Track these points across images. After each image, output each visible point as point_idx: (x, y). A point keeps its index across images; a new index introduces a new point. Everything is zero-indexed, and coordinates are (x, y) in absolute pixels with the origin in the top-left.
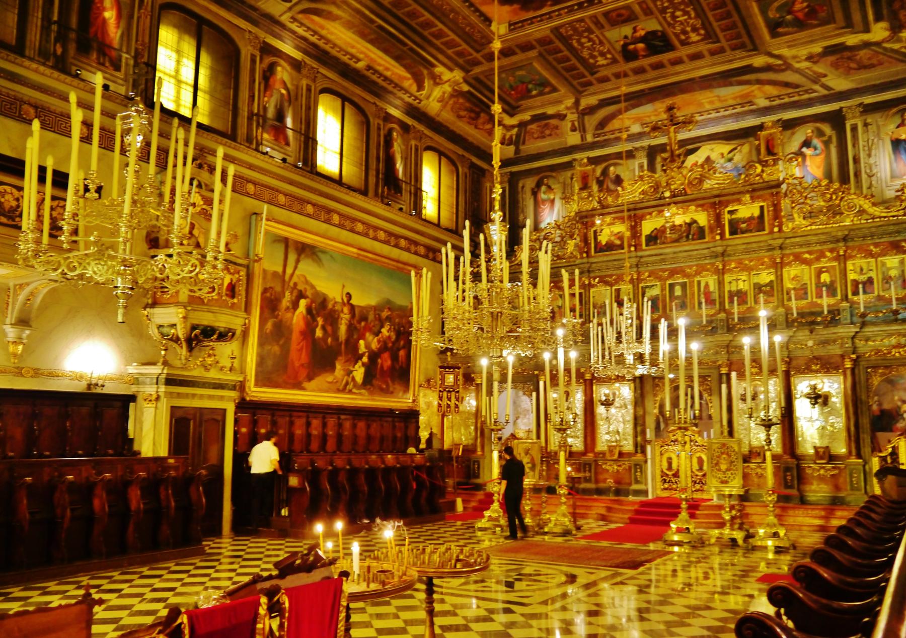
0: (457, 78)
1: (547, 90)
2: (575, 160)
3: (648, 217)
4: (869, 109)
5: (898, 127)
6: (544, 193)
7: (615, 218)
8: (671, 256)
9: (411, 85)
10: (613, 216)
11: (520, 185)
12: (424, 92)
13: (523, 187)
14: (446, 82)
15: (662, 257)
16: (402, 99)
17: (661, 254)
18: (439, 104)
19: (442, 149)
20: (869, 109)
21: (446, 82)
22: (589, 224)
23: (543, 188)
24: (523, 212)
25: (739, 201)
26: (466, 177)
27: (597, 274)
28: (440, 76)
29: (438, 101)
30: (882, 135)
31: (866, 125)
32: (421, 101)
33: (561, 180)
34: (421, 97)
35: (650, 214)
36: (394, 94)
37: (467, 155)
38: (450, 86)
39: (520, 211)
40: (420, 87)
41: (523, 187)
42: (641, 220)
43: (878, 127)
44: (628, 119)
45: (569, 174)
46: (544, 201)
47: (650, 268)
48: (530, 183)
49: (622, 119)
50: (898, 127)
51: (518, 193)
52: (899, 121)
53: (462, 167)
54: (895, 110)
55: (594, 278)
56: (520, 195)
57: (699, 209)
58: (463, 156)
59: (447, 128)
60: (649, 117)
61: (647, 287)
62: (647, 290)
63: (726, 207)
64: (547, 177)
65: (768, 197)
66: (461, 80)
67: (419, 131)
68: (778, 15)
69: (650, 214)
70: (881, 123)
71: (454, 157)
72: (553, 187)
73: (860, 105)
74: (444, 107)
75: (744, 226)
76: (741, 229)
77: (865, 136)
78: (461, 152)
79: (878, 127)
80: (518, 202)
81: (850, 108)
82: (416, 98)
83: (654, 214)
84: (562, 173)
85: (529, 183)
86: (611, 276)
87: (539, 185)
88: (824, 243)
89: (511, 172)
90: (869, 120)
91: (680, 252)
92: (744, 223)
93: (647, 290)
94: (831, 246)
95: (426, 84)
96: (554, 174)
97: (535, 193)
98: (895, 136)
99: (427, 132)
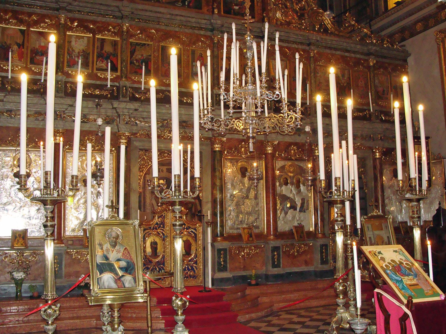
8: (169, 16)
15: (159, 15)
17: (156, 12)
27: (77, 15)
47: (142, 24)
55: (72, 20)
61: (137, 44)
62: (138, 47)
75: (237, 8)
76: (234, 10)
86: (94, 22)
88: (302, 43)
91: (177, 15)
92: (236, 5)
93: (138, 47)
94: (304, 47)
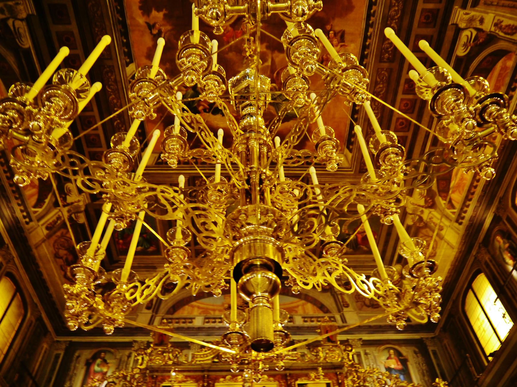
0: (81, 204)
1: (151, 249)
2: (135, 341)
3: (222, 379)
4: (367, 343)
5: (388, 359)
6: (98, 365)
7: (186, 377)
9: (32, 196)
10: (186, 374)
11: (77, 354)
12: (40, 210)
13: (78, 357)
14: (68, 205)
16: (13, 212)
18: (46, 232)
19: (22, 286)
20: (367, 343)
21: (68, 205)
22: (159, 378)
23: (99, 361)
24: (70, 380)
25: (308, 377)
26: (31, 325)
28: (66, 195)
29: (47, 228)
30: (379, 363)
31: (366, 354)
32: (31, 220)
33: (118, 357)
34: (33, 216)
35: (224, 377)
36: (8, 201)
37: (39, 304)
38: (69, 211)
39: (68, 378)
40: (39, 203)
41: (78, 357)
42: (215, 382)
43: (375, 357)
44: (199, 308)
45: (127, 352)
46: (96, 373)
48: (87, 354)
49: (193, 307)
50: (388, 359)
51: (71, 362)
52: (388, 356)
53: (32, 314)
54: (383, 347)
56: (73, 364)
57: (271, 379)
58: (36, 305)
59: (37, 266)
60: (214, 310)
63: (297, 380)
64: (105, 352)
65: (332, 375)
66: (83, 209)
67: (10, 254)
68: (347, 232)
69: (224, 377)
70: (376, 354)
71: (28, 300)
72: (108, 361)
73: (360, 339)
74: (48, 237)
77: (367, 361)
78: (36, 300)
79: (375, 357)
80: (68, 369)
81: (353, 340)
82: (28, 216)
83: (228, 377)
84: (120, 351)
85: (87, 354)
87: (94, 358)
89: (71, 342)
90: (368, 351)
95: (47, 201)
96: (112, 350)
97: (89, 364)
98: (387, 365)
99: (17, 261)
